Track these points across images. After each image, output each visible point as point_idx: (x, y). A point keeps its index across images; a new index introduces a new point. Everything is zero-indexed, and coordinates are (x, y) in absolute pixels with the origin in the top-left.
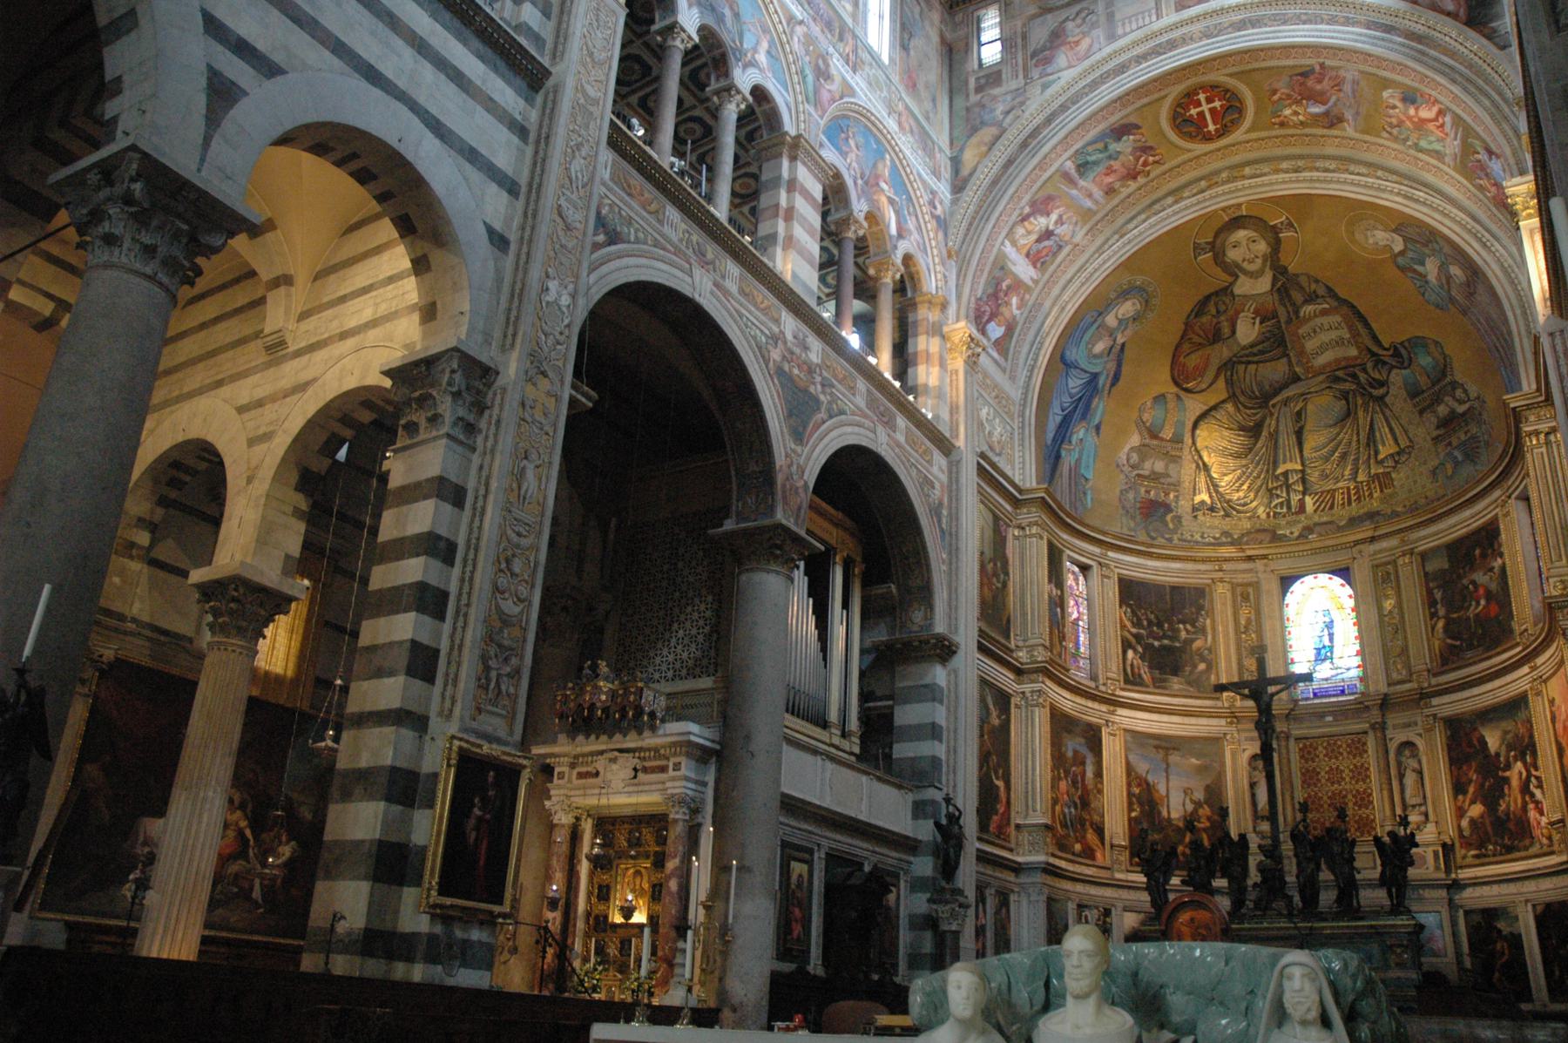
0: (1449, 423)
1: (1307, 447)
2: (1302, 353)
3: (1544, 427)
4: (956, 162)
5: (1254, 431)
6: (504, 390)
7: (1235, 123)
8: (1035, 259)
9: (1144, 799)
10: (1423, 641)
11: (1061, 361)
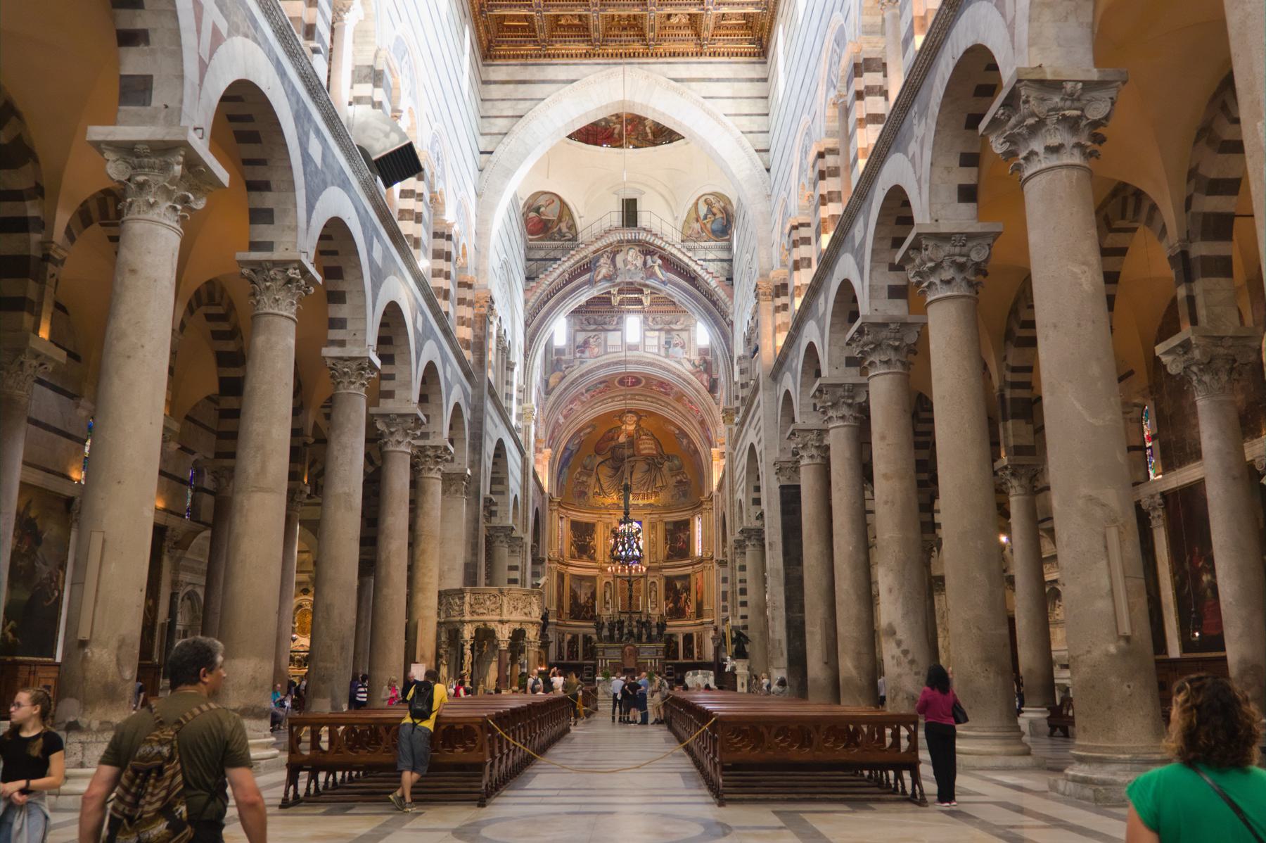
0: (680, 482)
1: (634, 477)
2: (638, 448)
3: (708, 507)
4: (547, 382)
5: (616, 469)
6: (526, 544)
7: (637, 385)
8: (565, 417)
9: (574, 597)
10: (662, 550)
11: (566, 448)
